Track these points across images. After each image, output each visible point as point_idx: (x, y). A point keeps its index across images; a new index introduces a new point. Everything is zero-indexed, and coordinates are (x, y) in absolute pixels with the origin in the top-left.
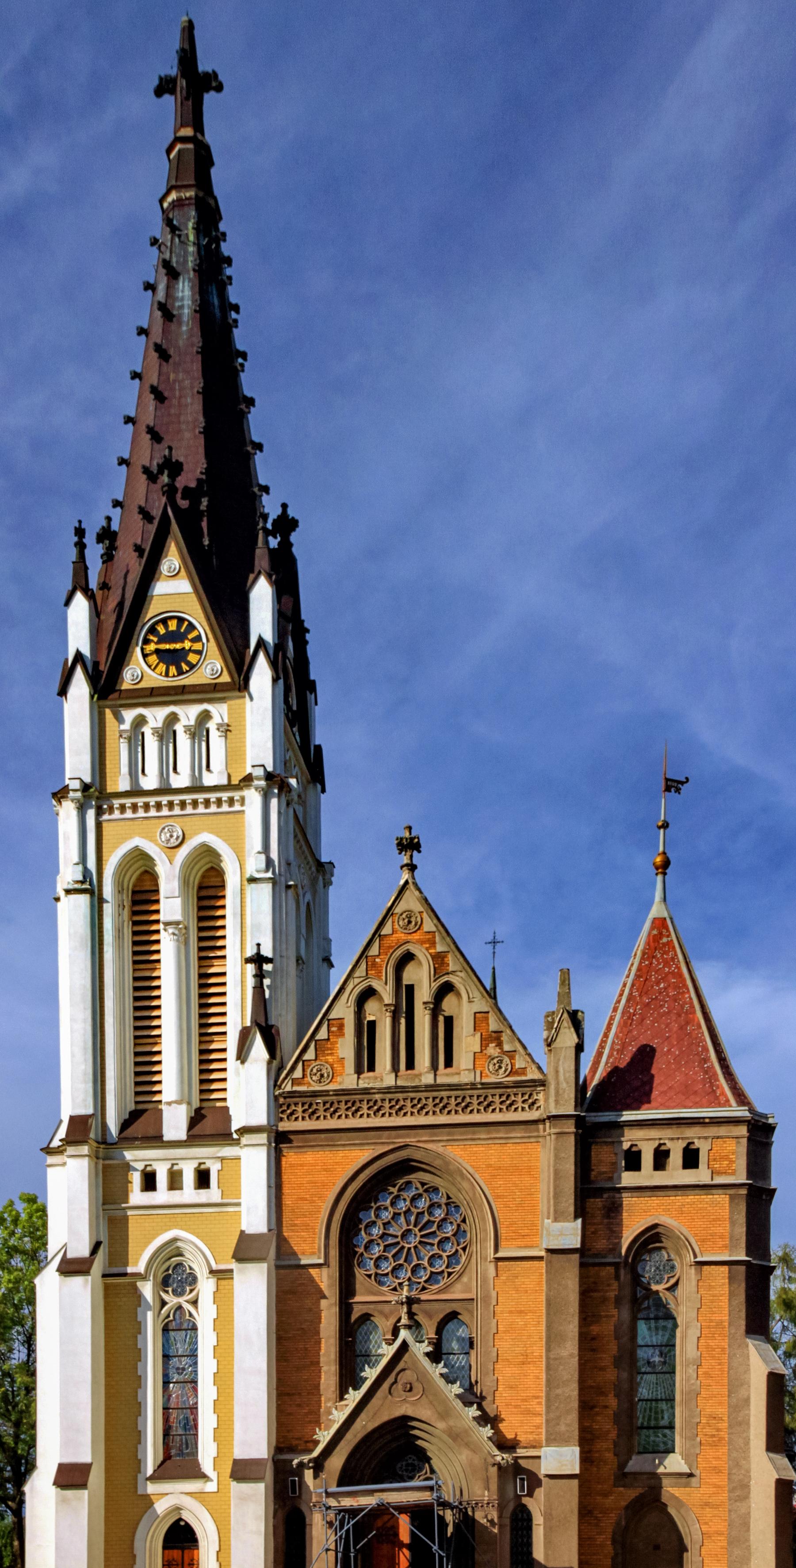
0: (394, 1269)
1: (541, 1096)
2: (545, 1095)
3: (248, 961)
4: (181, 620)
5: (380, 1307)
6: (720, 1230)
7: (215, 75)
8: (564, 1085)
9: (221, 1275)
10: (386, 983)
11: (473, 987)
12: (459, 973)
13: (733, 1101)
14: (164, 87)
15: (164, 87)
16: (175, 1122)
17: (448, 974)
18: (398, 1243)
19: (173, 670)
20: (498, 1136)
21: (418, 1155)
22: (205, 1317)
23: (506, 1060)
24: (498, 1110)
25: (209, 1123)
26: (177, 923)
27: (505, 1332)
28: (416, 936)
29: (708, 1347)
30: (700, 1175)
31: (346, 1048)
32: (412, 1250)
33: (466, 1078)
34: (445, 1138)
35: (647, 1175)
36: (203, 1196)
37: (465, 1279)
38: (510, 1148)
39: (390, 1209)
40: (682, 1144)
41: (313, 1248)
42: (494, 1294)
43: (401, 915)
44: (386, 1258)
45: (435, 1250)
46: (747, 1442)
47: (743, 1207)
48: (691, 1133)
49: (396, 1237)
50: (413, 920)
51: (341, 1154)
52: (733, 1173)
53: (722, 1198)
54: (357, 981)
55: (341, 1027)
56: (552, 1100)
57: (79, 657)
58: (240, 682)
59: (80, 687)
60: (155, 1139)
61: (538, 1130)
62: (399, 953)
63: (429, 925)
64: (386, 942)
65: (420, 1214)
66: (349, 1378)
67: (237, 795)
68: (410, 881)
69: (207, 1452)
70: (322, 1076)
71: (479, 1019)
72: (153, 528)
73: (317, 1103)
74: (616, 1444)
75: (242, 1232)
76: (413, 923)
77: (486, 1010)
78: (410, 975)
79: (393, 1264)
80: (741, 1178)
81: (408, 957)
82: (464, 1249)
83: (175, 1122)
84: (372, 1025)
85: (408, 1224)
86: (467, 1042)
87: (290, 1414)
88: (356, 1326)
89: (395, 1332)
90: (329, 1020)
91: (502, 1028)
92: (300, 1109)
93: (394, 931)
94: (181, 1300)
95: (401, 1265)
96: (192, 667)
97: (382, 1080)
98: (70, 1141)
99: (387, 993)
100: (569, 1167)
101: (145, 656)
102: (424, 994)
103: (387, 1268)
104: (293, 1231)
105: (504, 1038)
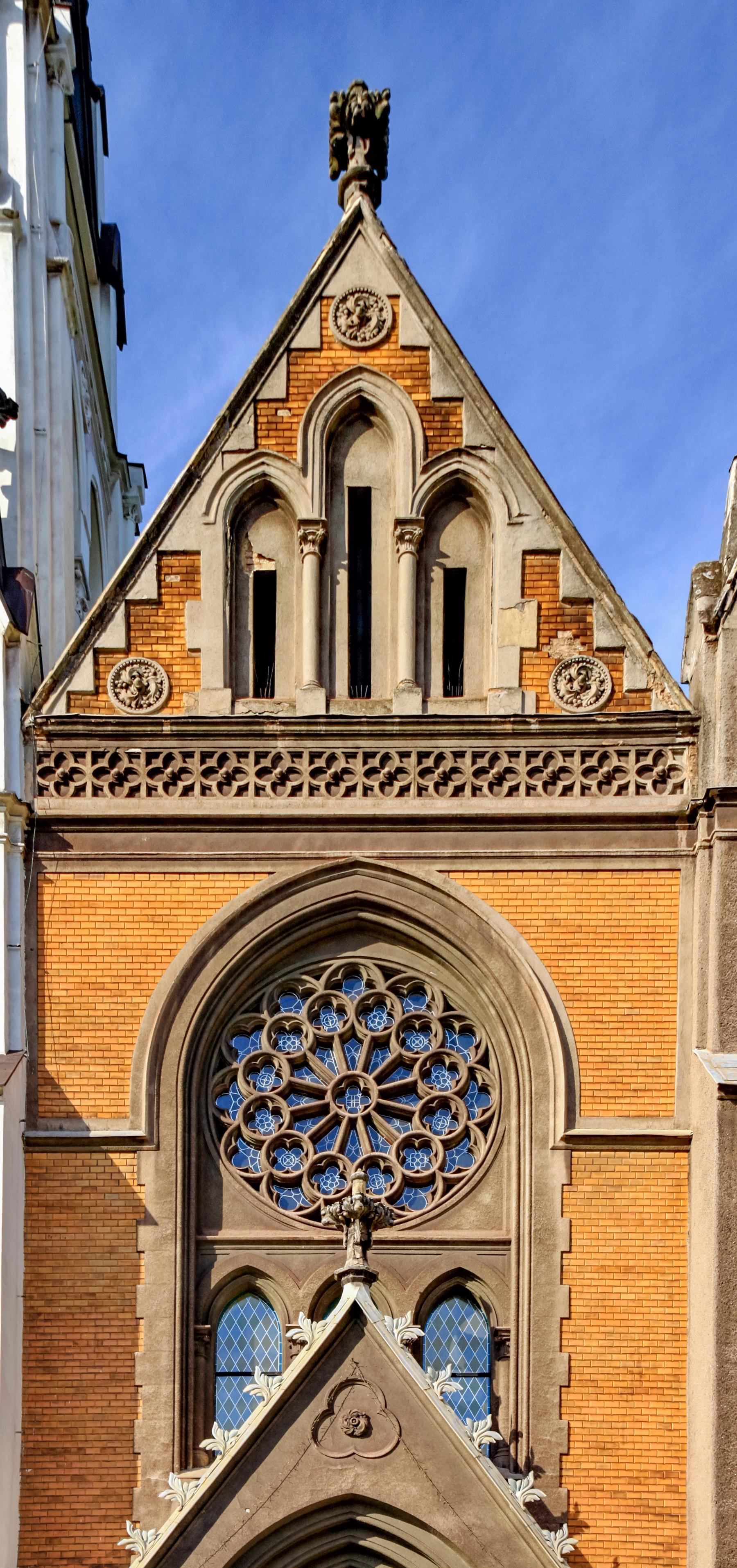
0: (316, 1170)
1: (684, 761)
2: (695, 755)
10: (304, 470)
11: (522, 488)
12: (485, 454)
17: (459, 452)
18: (325, 1109)
20: (577, 850)
23: (600, 670)
24: (577, 789)
27: (588, 1316)
28: (377, 359)
31: (203, 623)
32: (360, 1125)
33: (500, 705)
34: (447, 852)
39: (308, 1028)
42: (562, 1226)
43: (344, 299)
45: (416, 1126)
49: (319, 1094)
50: (373, 314)
51: (189, 882)
54: (231, 460)
55: (191, 574)
61: (674, 842)
62: (338, 395)
65: (380, 1044)
68: (366, 211)
71: (537, 562)
73: (132, 756)
76: (373, 323)
77: (551, 545)
79: (312, 1157)
81: (360, 414)
85: (351, 1063)
87: (57, 1499)
88: (220, 1301)
90: (161, 554)
91: (593, 591)
95: (332, 1162)
97: (293, 706)
99: (305, 497)
103: (297, 1167)
104: (69, 1061)
105: (596, 616)
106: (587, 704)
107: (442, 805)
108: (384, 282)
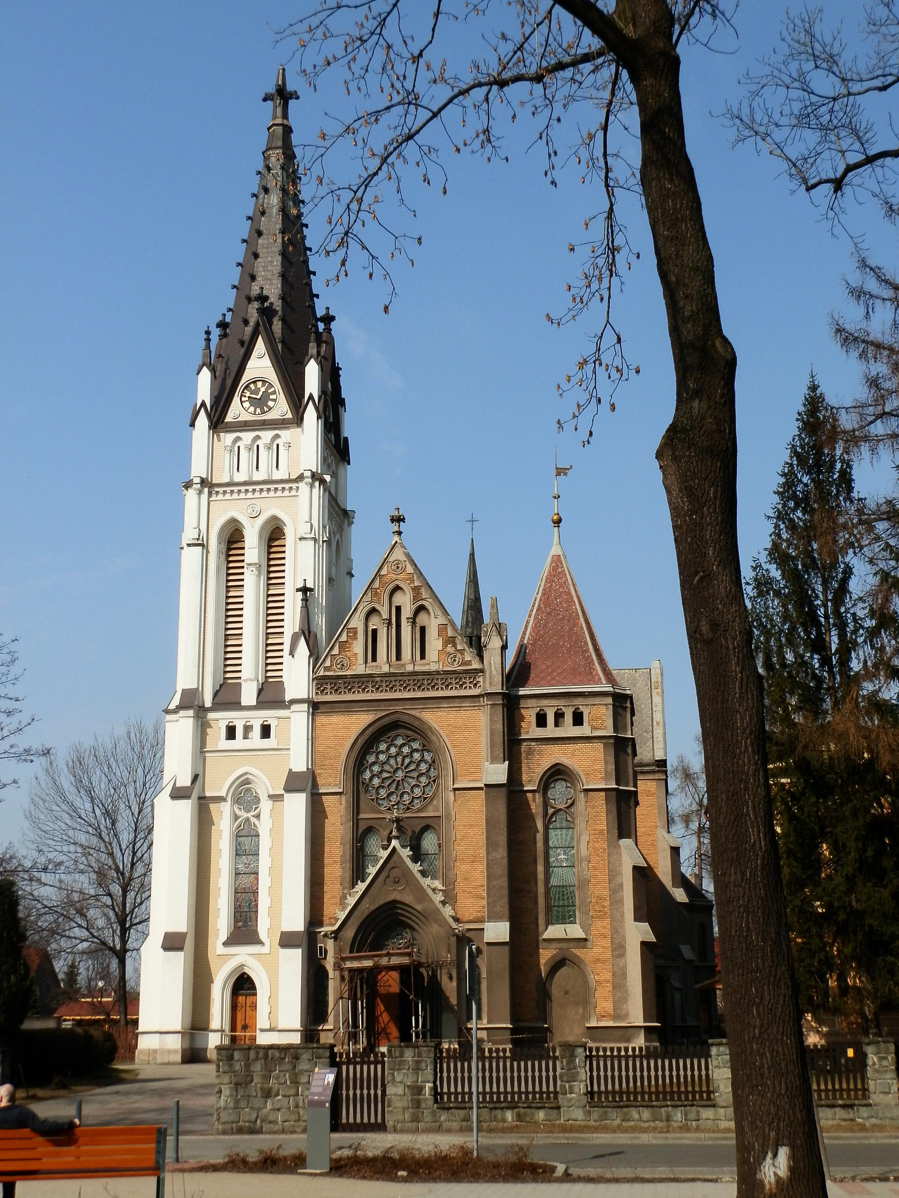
3: (298, 590)
5: (379, 821)
6: (599, 767)
9: (276, 798)
19: (258, 410)
21: (404, 718)
22: (264, 827)
25: (271, 695)
26: (255, 564)
28: (402, 576)
29: (594, 848)
31: (358, 647)
33: (433, 667)
35: (551, 731)
37: (435, 802)
40: (572, 709)
41: (333, 781)
42: (453, 813)
44: (383, 787)
46: (622, 916)
47: (612, 751)
48: (578, 701)
51: (354, 717)
52: (605, 728)
53: (599, 746)
54: (366, 604)
55: (355, 633)
57: (203, 404)
58: (298, 420)
59: (203, 421)
60: (236, 705)
62: (392, 586)
64: (384, 579)
66: (358, 874)
67: (294, 485)
69: (263, 926)
70: (343, 665)
71: (442, 629)
72: (249, 330)
75: (290, 770)
78: (398, 599)
80: (610, 732)
81: (397, 588)
82: (434, 781)
84: (375, 632)
86: (434, 644)
89: (389, 841)
92: (329, 687)
93: (388, 573)
94: (249, 815)
98: (181, 707)
101: (242, 402)
102: (407, 613)
106: (456, 667)
107: (419, 694)
108: (403, 558)
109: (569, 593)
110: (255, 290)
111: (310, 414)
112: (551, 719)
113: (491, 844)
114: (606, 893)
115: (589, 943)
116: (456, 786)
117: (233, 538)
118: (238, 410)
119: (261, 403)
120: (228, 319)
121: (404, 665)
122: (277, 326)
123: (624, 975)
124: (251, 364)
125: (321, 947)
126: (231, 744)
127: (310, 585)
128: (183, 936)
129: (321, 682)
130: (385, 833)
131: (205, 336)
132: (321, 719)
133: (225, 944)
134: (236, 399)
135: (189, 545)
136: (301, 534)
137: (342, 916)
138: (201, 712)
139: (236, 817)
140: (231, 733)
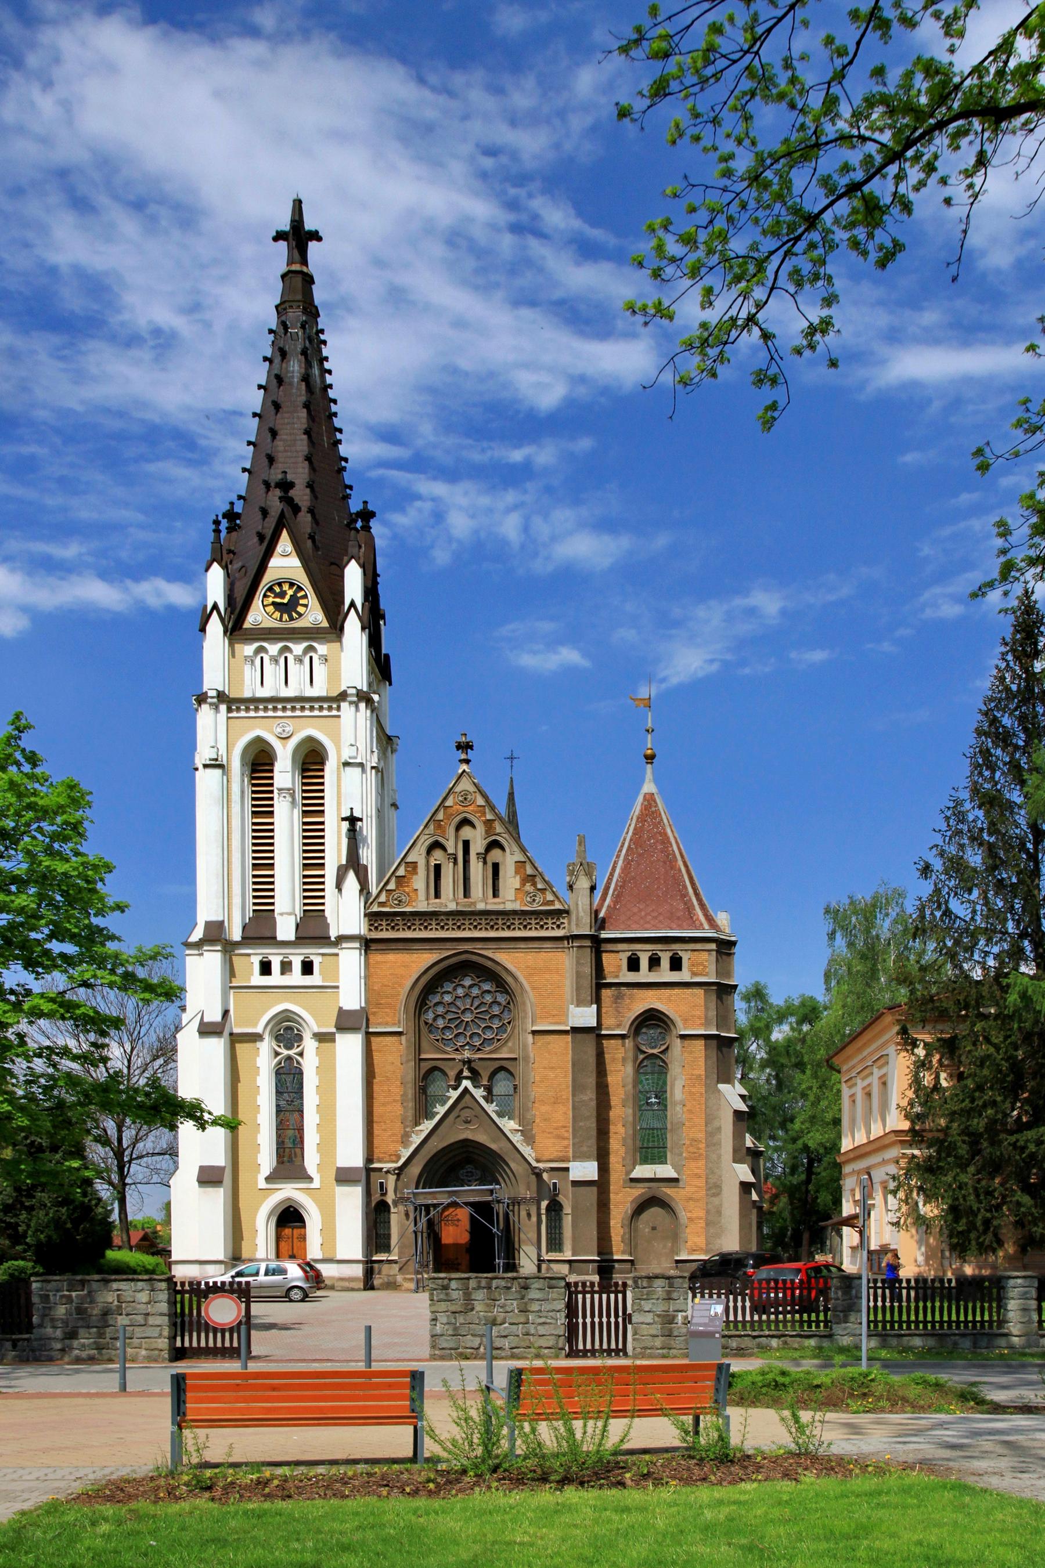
3: (344, 819)
4: (292, 585)
7: (317, 232)
8: (581, 914)
9: (323, 1038)
13: (706, 926)
14: (279, 236)
15: (279, 236)
16: (286, 930)
19: (285, 617)
22: (310, 1064)
25: (313, 930)
29: (691, 1093)
30: (684, 976)
35: (644, 975)
36: (308, 980)
38: (543, 955)
46: (719, 1157)
47: (714, 997)
53: (700, 992)
56: (574, 923)
57: (215, 607)
58: (336, 629)
59: (215, 626)
60: (271, 940)
63: (480, 801)
69: (311, 1160)
74: (624, 1159)
75: (340, 1008)
83: (286, 930)
89: (459, 1078)
94: (291, 1052)
96: (300, 615)
100: (588, 969)
109: (666, 834)
110: (276, 476)
111: (353, 625)
112: (644, 963)
113: (577, 1088)
114: (701, 1136)
115: (681, 1184)
116: (535, 1028)
117: (259, 761)
118: (259, 615)
119: (289, 608)
120: (238, 508)
121: (474, 904)
122: (305, 518)
123: (719, 1213)
124: (274, 562)
125: (381, 1184)
126: (266, 981)
127: (357, 814)
128: (221, 1169)
129: (373, 918)
130: (452, 1074)
131: (213, 527)
132: (376, 957)
133: (268, 1179)
134: (257, 602)
135: (205, 766)
136: (345, 757)
137: (406, 1154)
138: (229, 948)
139: (277, 1054)
140: (266, 968)
